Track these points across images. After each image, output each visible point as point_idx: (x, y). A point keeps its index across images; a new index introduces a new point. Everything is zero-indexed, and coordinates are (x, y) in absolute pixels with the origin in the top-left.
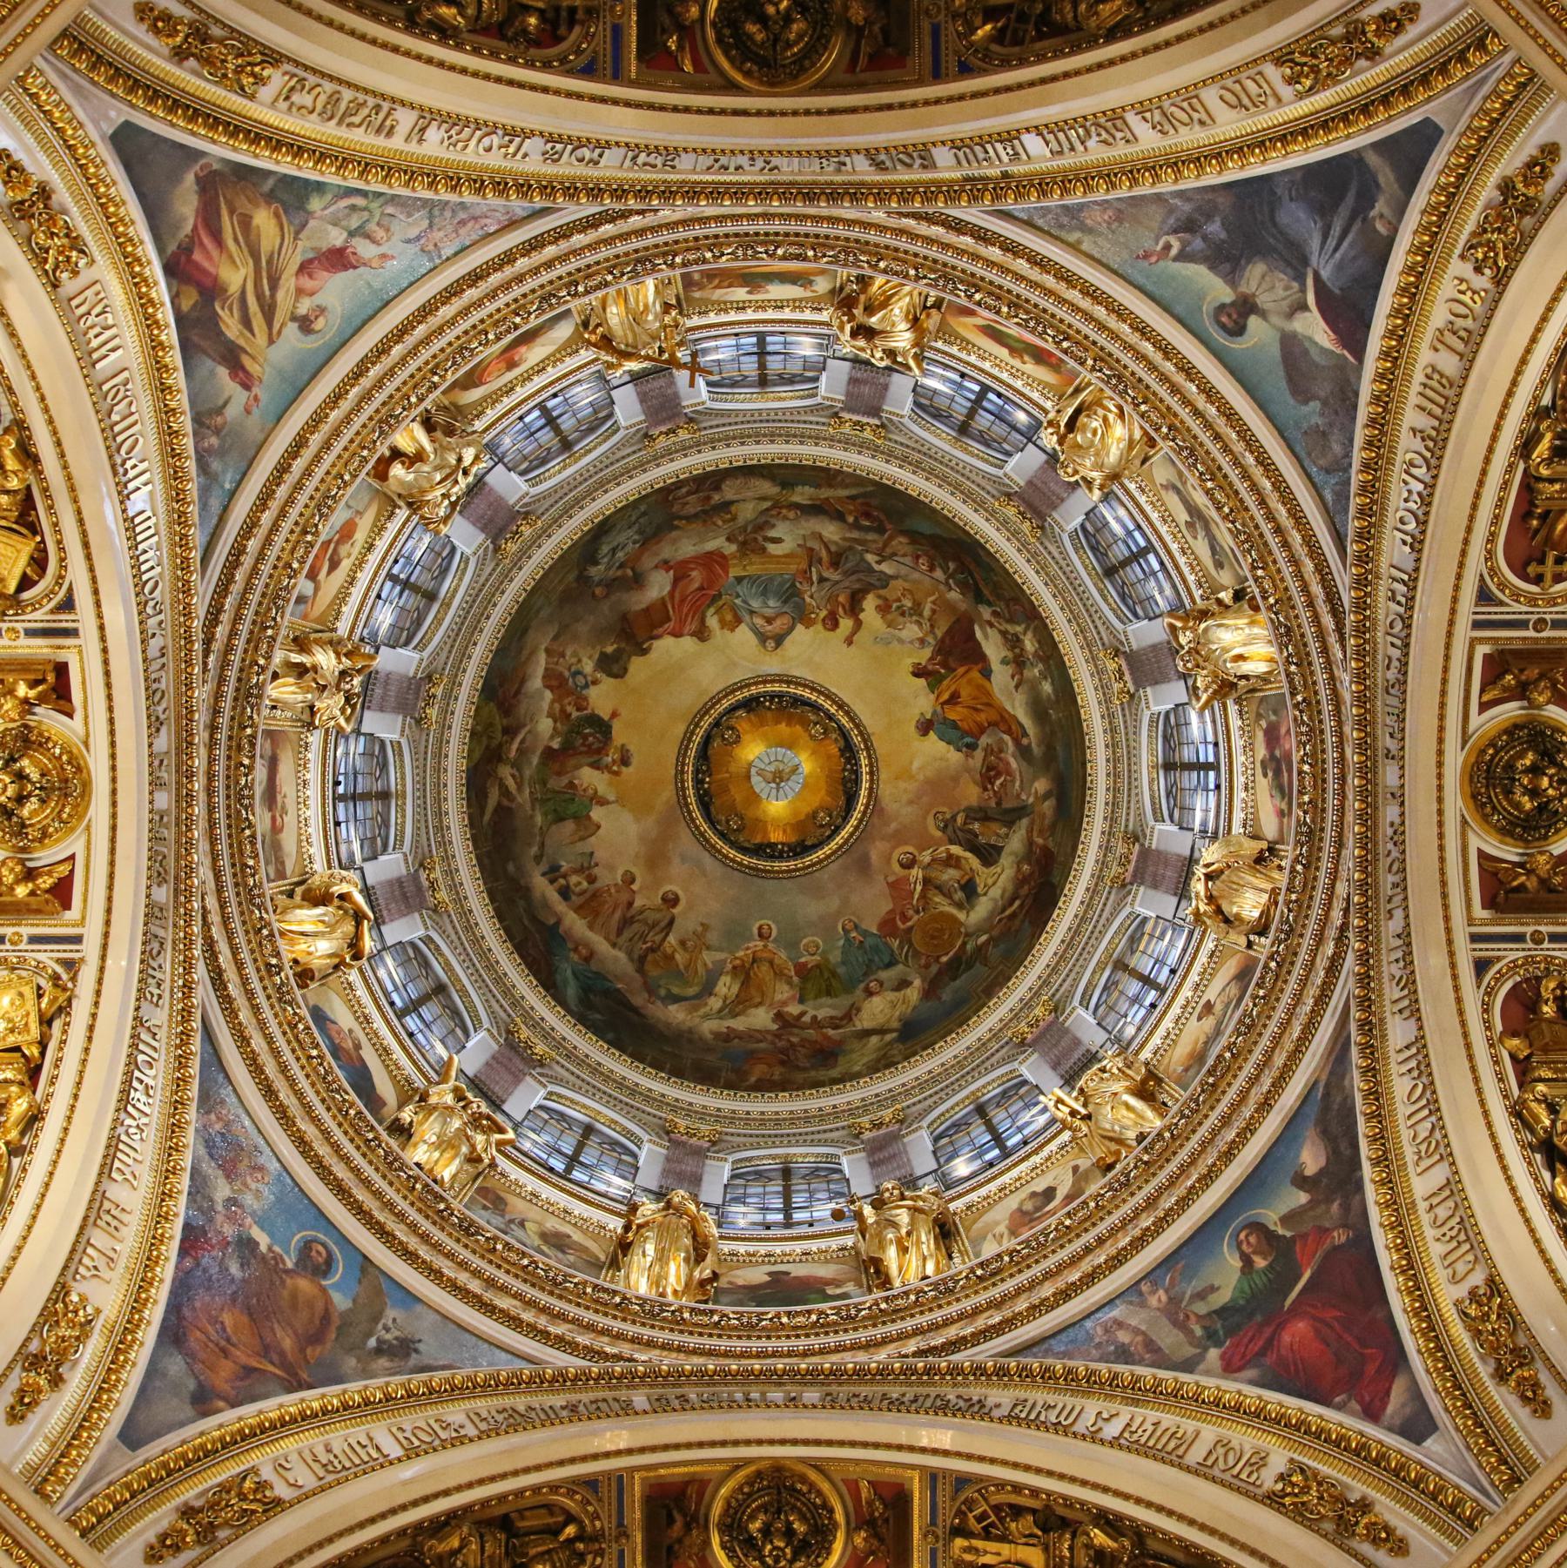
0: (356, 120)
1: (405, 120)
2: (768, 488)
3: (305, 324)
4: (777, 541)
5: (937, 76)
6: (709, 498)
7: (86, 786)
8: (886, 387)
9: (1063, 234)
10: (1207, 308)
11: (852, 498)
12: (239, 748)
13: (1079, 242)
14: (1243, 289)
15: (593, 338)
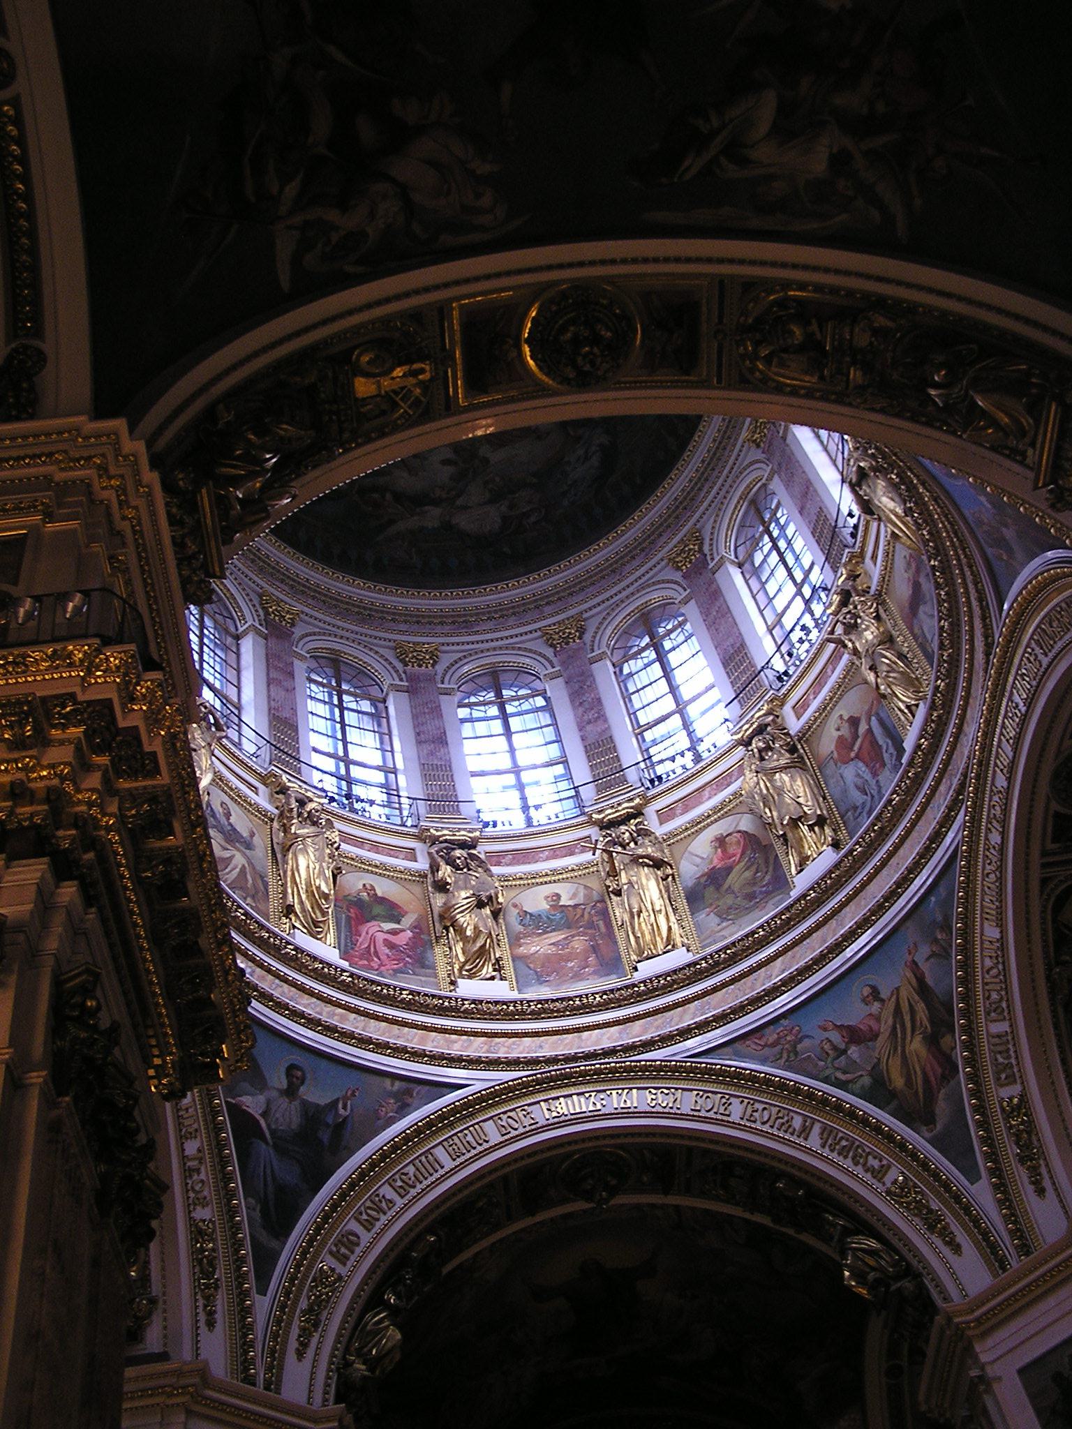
0: (844, 1143)
1: (814, 1141)
2: (463, 521)
3: (875, 994)
4: (446, 462)
5: (505, 1178)
6: (511, 507)
7: (1056, 775)
8: (419, 742)
9: (404, 1085)
10: (308, 1076)
11: (392, 522)
12: (943, 705)
13: (392, 1085)
14: (297, 1103)
15: (669, 871)
